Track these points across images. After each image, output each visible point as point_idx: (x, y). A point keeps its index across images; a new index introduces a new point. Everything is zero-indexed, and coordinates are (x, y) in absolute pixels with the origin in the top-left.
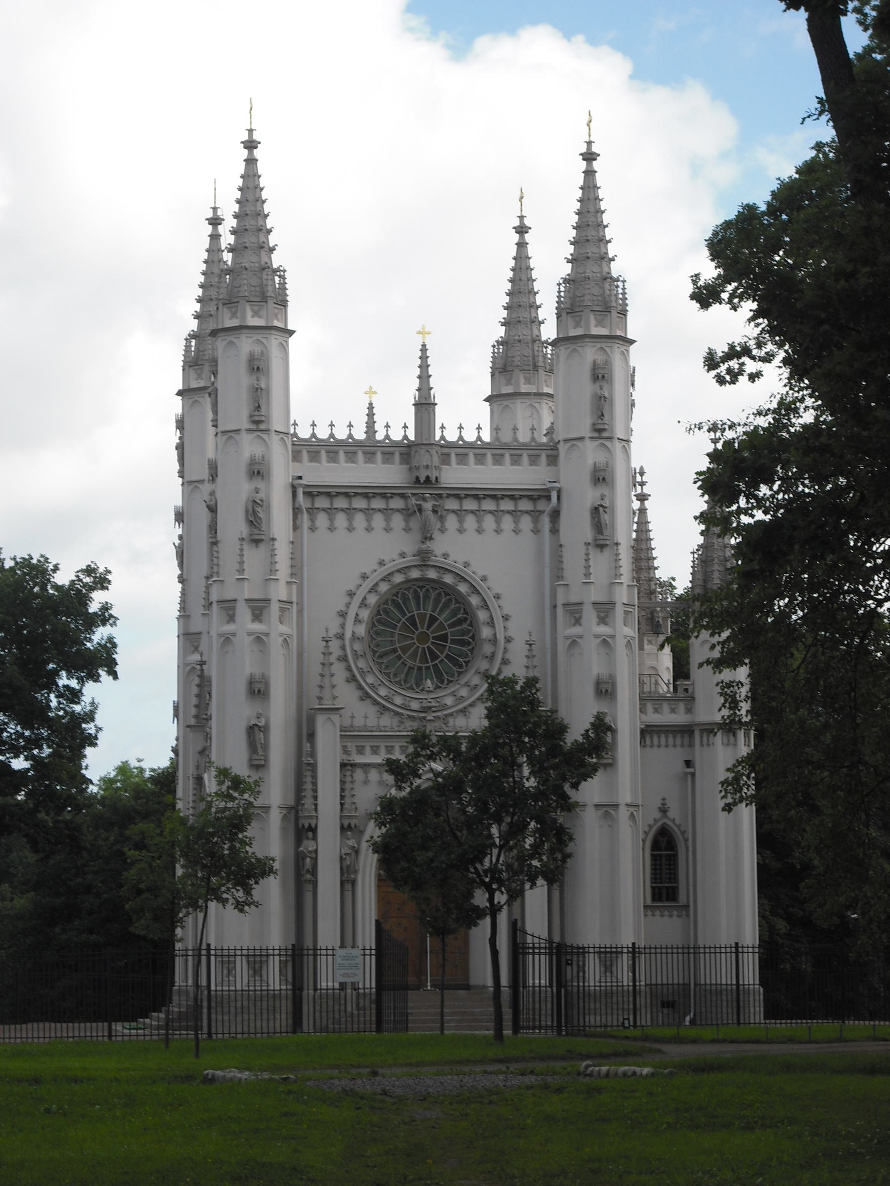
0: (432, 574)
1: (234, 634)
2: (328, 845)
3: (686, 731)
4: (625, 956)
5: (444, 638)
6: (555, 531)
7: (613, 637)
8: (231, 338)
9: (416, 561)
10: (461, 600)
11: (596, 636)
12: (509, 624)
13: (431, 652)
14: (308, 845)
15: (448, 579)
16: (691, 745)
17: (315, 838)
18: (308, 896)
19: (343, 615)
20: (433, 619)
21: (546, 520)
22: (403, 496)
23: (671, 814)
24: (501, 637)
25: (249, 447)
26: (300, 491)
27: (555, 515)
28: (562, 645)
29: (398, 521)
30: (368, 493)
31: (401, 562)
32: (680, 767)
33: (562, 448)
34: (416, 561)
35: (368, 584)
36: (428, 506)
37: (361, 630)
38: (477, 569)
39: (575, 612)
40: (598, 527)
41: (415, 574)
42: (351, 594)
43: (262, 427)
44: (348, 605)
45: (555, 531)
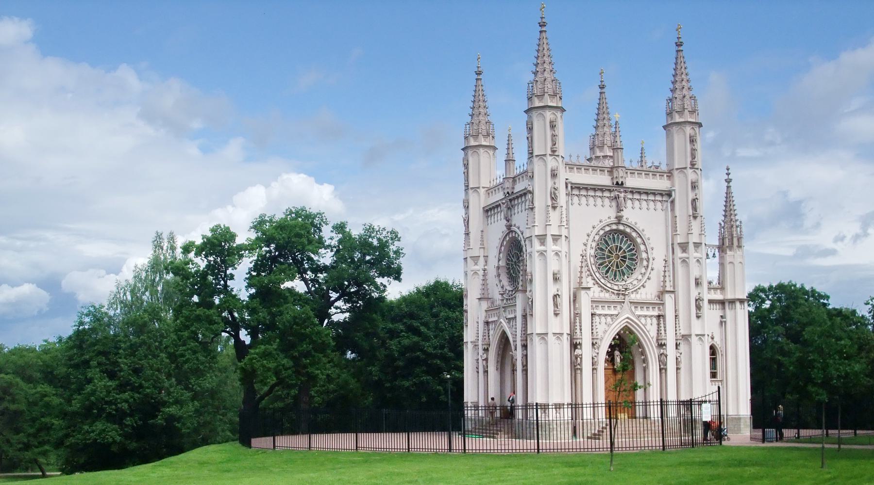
0: (621, 227)
1: (546, 251)
2: (586, 352)
3: (722, 303)
6: (673, 210)
8: (541, 112)
9: (615, 221)
10: (632, 240)
12: (654, 251)
14: (578, 352)
15: (628, 230)
16: (724, 308)
17: (581, 349)
18: (579, 376)
20: (621, 248)
22: (610, 191)
25: (551, 163)
26: (569, 186)
27: (673, 202)
28: (678, 262)
29: (607, 201)
30: (595, 188)
31: (609, 221)
32: (719, 319)
33: (675, 173)
34: (615, 221)
36: (622, 195)
37: (592, 252)
38: (640, 227)
39: (684, 247)
40: (695, 208)
41: (614, 227)
43: (556, 154)
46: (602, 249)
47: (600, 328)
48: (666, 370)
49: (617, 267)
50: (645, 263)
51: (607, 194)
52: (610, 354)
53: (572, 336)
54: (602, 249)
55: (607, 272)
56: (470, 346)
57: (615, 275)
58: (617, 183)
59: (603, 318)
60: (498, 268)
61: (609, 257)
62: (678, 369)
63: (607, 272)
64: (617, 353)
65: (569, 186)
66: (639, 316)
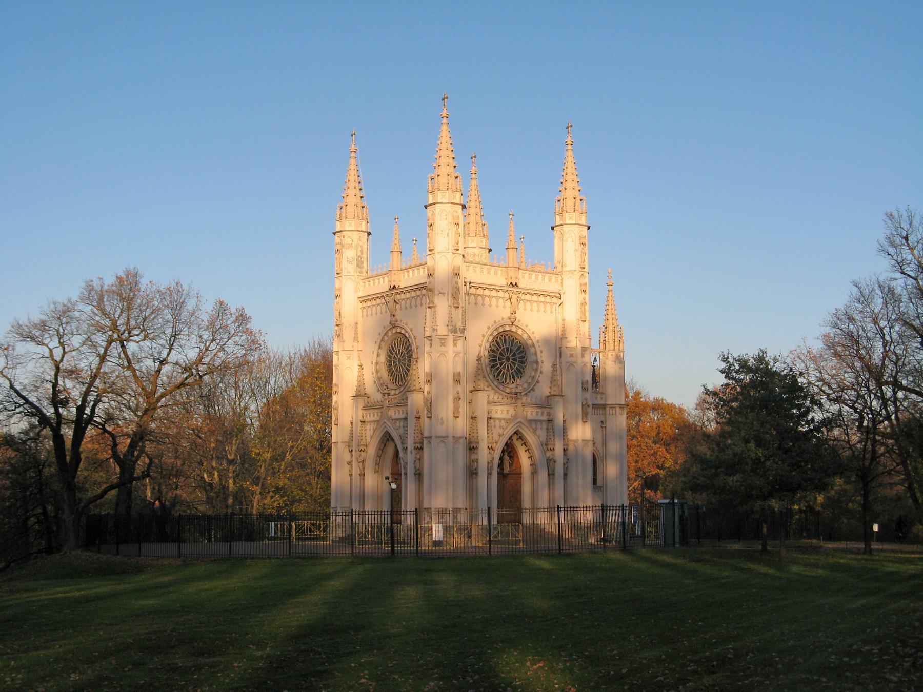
0: (514, 329)
24: (539, 360)
41: (507, 328)
46: (493, 351)
47: (496, 431)
48: (553, 474)
49: (508, 370)
50: (535, 366)
51: (501, 294)
52: (501, 459)
54: (493, 351)
55: (499, 374)
56: (341, 446)
57: (506, 379)
60: (377, 363)
61: (500, 359)
62: (565, 475)
63: (499, 374)
64: (506, 457)
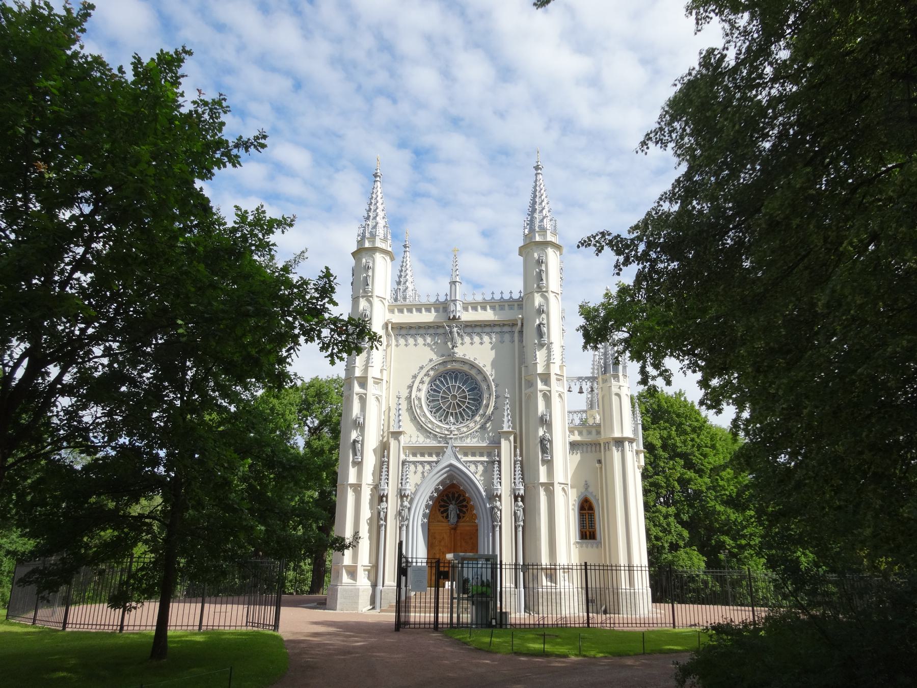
0: (456, 366)
4: (575, 571)
5: (465, 397)
6: (521, 341)
7: (550, 391)
11: (541, 391)
13: (458, 404)
14: (384, 505)
19: (411, 387)
21: (516, 335)
23: (590, 490)
26: (390, 326)
27: (521, 332)
31: (441, 360)
35: (424, 371)
42: (415, 377)
44: (413, 382)
45: (521, 341)
53: (376, 487)
58: (449, 319)
59: (420, 468)
65: (390, 326)
66: (466, 462)
